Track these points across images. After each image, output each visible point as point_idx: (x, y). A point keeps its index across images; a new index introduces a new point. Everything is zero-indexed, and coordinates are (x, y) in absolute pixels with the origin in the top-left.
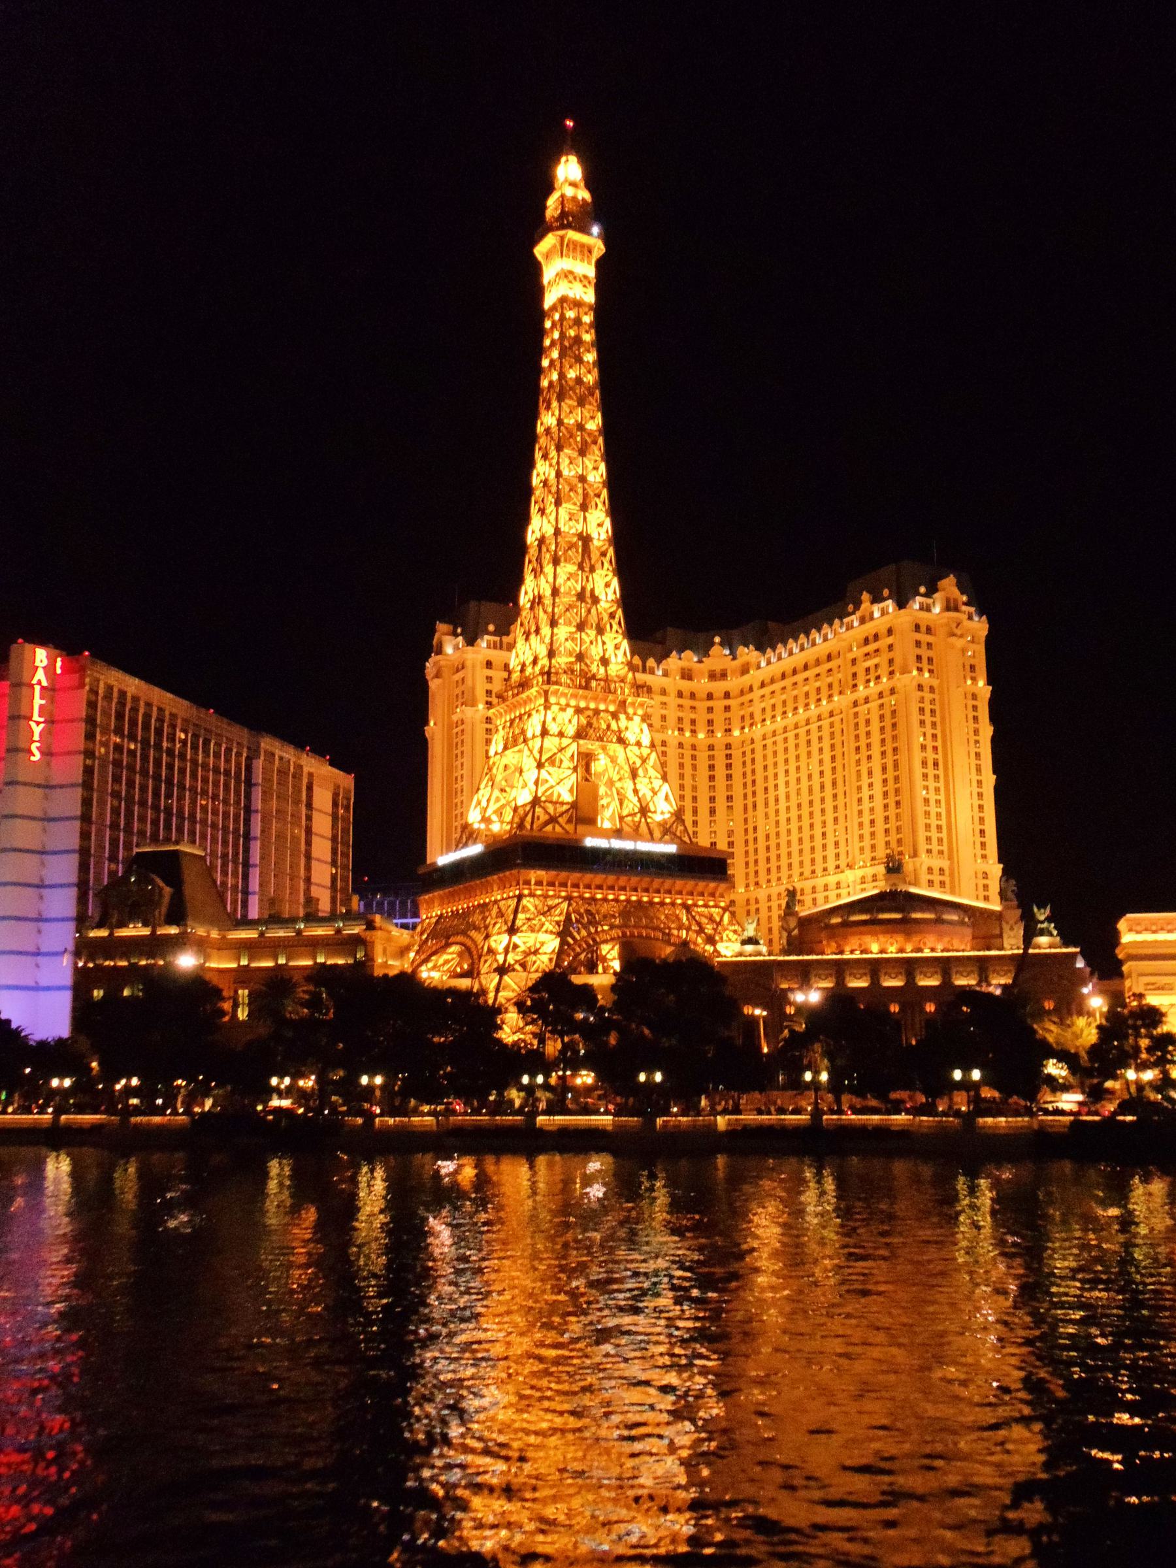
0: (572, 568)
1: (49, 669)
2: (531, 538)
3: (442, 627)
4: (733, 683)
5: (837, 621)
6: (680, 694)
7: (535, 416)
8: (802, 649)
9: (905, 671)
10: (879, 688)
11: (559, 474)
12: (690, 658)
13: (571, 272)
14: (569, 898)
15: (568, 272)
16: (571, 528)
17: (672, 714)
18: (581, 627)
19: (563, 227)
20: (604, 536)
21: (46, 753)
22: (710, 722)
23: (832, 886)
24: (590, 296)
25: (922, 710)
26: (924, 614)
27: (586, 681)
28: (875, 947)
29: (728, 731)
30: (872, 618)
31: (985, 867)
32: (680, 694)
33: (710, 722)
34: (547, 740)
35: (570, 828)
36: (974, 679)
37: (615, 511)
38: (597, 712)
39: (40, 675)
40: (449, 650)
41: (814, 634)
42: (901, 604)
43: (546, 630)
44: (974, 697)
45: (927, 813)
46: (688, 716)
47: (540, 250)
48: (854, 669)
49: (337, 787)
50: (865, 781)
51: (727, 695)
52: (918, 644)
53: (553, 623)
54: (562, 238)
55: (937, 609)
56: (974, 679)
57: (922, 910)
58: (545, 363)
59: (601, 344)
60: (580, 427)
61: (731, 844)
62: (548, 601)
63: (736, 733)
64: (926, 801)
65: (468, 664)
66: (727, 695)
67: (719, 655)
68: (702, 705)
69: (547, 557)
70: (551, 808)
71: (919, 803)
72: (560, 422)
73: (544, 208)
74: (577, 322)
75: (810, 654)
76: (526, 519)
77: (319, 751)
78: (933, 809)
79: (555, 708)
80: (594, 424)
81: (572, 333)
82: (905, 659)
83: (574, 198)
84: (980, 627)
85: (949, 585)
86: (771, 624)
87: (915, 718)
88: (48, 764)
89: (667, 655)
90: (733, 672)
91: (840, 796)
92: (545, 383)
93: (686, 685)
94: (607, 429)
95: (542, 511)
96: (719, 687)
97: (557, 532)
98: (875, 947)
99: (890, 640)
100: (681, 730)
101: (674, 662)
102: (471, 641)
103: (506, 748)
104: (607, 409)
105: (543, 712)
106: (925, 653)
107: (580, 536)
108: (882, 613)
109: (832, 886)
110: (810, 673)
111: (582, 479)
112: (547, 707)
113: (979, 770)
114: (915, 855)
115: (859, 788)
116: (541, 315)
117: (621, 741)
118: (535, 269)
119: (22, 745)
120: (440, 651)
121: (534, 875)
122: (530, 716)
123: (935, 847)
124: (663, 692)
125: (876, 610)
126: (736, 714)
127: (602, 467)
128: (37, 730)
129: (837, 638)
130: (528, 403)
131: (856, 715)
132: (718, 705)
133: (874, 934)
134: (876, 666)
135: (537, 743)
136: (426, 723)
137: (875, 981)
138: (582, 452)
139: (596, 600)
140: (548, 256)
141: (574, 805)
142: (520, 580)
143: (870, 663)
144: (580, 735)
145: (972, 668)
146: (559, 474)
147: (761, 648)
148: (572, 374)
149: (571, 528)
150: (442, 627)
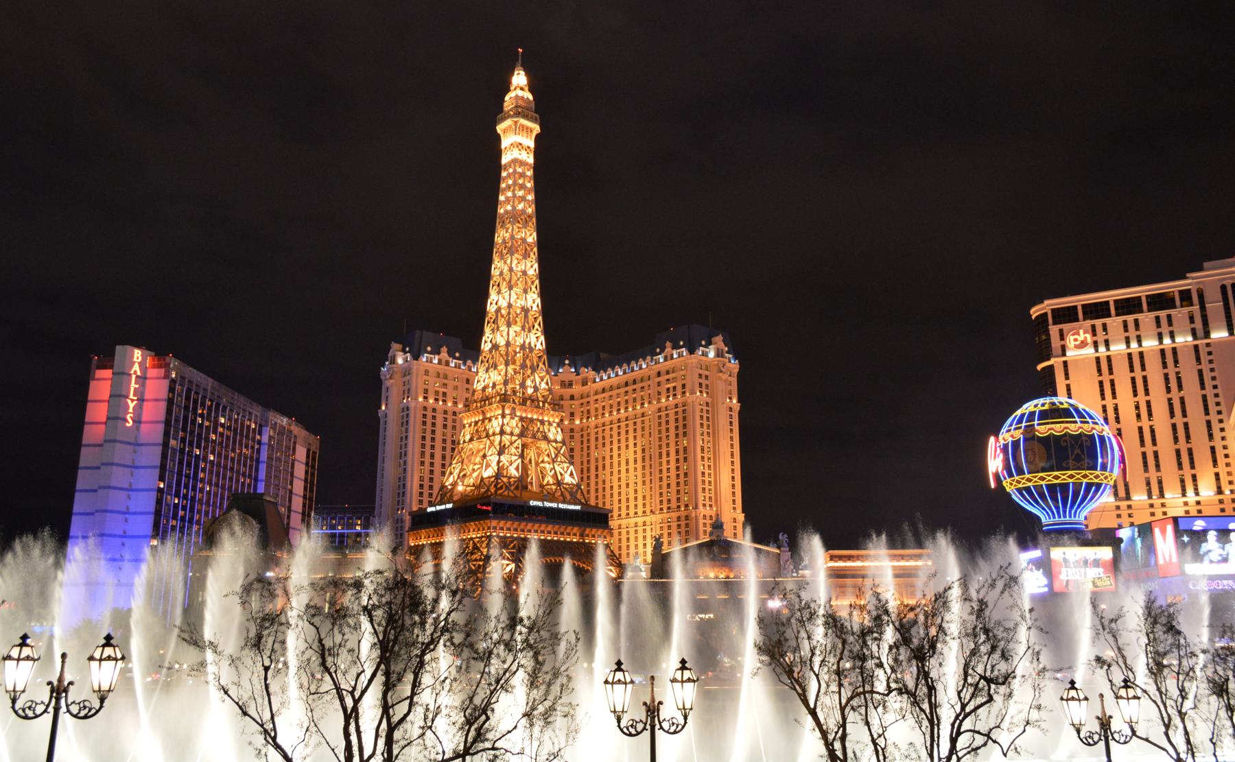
0: (517, 328)
2: (491, 308)
3: (395, 346)
4: (577, 389)
5: (649, 358)
8: (625, 373)
9: (693, 393)
10: (676, 401)
11: (511, 270)
15: (517, 143)
19: (518, 114)
20: (535, 308)
21: (137, 421)
23: (640, 524)
24: (531, 160)
25: (702, 417)
26: (704, 358)
28: (712, 575)
30: (672, 358)
31: (735, 515)
35: (518, 493)
37: (543, 295)
38: (532, 420)
39: (136, 367)
40: (400, 361)
41: (633, 364)
42: (692, 351)
43: (501, 367)
44: (731, 409)
45: (703, 481)
48: (659, 389)
50: (664, 459)
51: (572, 398)
54: (516, 122)
55: (712, 355)
58: (502, 198)
60: (524, 240)
62: (503, 350)
63: (578, 422)
64: (703, 473)
65: (414, 371)
66: (572, 398)
69: (501, 321)
70: (505, 480)
71: (700, 475)
72: (512, 237)
73: (503, 101)
75: (630, 376)
76: (486, 295)
78: (707, 479)
80: (532, 238)
81: (521, 181)
82: (693, 383)
83: (522, 98)
84: (734, 365)
85: (719, 340)
86: (603, 355)
87: (698, 421)
88: (138, 429)
90: (577, 383)
91: (647, 467)
92: (501, 211)
95: (499, 292)
97: (510, 306)
99: (683, 373)
102: (416, 357)
103: (471, 440)
105: (500, 419)
106: (704, 382)
107: (523, 308)
108: (678, 356)
109: (640, 524)
110: (630, 388)
111: (524, 273)
112: (503, 416)
113: (732, 455)
114: (696, 507)
115: (661, 464)
116: (498, 167)
118: (497, 139)
119: (121, 415)
120: (393, 361)
122: (490, 420)
123: (708, 503)
127: (536, 266)
128: (132, 405)
130: (487, 220)
131: (660, 417)
134: (675, 388)
135: (498, 438)
136: (380, 408)
138: (526, 256)
139: (531, 350)
140: (504, 131)
142: (482, 333)
143: (670, 386)
144: (521, 435)
146: (511, 270)
150: (395, 346)
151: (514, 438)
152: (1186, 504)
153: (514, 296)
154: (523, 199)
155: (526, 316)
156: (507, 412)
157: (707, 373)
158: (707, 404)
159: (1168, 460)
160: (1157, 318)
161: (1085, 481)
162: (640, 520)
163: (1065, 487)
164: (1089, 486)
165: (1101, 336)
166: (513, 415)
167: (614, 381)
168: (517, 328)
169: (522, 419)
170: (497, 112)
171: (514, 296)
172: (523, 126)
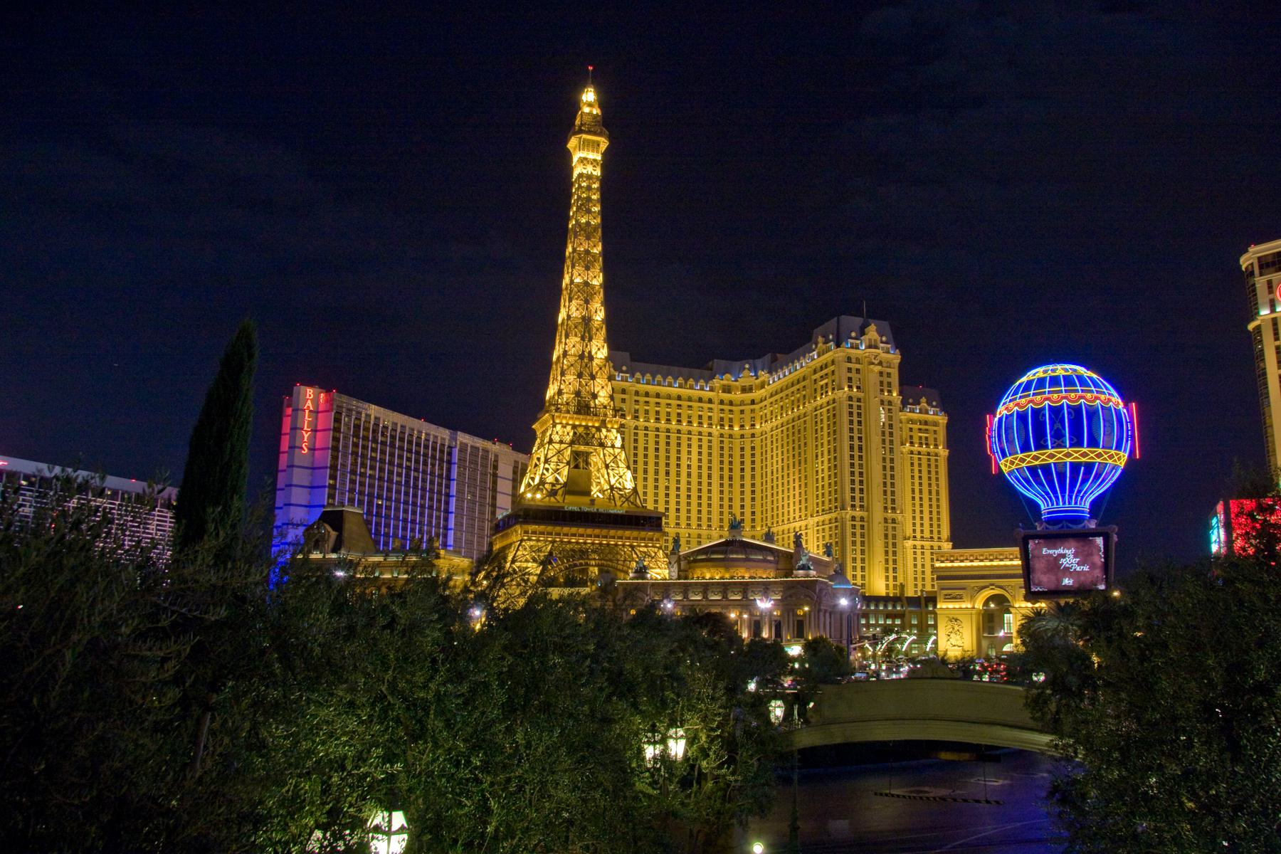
1: (316, 400)
9: (841, 388)
12: (728, 379)
13: (586, 159)
14: (553, 542)
15: (586, 158)
21: (312, 449)
25: (851, 414)
26: (853, 351)
28: (708, 576)
29: (753, 425)
32: (722, 402)
36: (890, 392)
37: (607, 303)
38: (587, 427)
42: (838, 345)
46: (726, 416)
49: (516, 462)
51: (753, 402)
56: (890, 392)
57: (737, 553)
59: (604, 201)
60: (587, 252)
61: (667, 509)
63: (758, 427)
66: (753, 402)
67: (747, 378)
74: (589, 188)
77: (504, 440)
79: (559, 427)
80: (597, 250)
83: (590, 114)
84: (895, 358)
85: (872, 333)
89: (712, 377)
93: (726, 396)
94: (605, 253)
98: (708, 576)
99: (832, 368)
100: (722, 426)
101: (717, 382)
104: (605, 240)
106: (853, 375)
107: (583, 318)
111: (586, 284)
117: (602, 445)
118: (568, 155)
121: (531, 528)
123: (857, 503)
124: (710, 401)
133: (708, 567)
137: (705, 597)
138: (587, 268)
139: (591, 358)
141: (565, 484)
143: (823, 382)
144: (572, 443)
145: (889, 384)
149: (575, 314)
151: (563, 446)
153: (573, 308)
157: (858, 366)
158: (859, 400)
161: (1069, 460)
163: (1046, 469)
164: (1075, 467)
167: (784, 382)
168: (574, 340)
171: (573, 308)
172: (589, 141)
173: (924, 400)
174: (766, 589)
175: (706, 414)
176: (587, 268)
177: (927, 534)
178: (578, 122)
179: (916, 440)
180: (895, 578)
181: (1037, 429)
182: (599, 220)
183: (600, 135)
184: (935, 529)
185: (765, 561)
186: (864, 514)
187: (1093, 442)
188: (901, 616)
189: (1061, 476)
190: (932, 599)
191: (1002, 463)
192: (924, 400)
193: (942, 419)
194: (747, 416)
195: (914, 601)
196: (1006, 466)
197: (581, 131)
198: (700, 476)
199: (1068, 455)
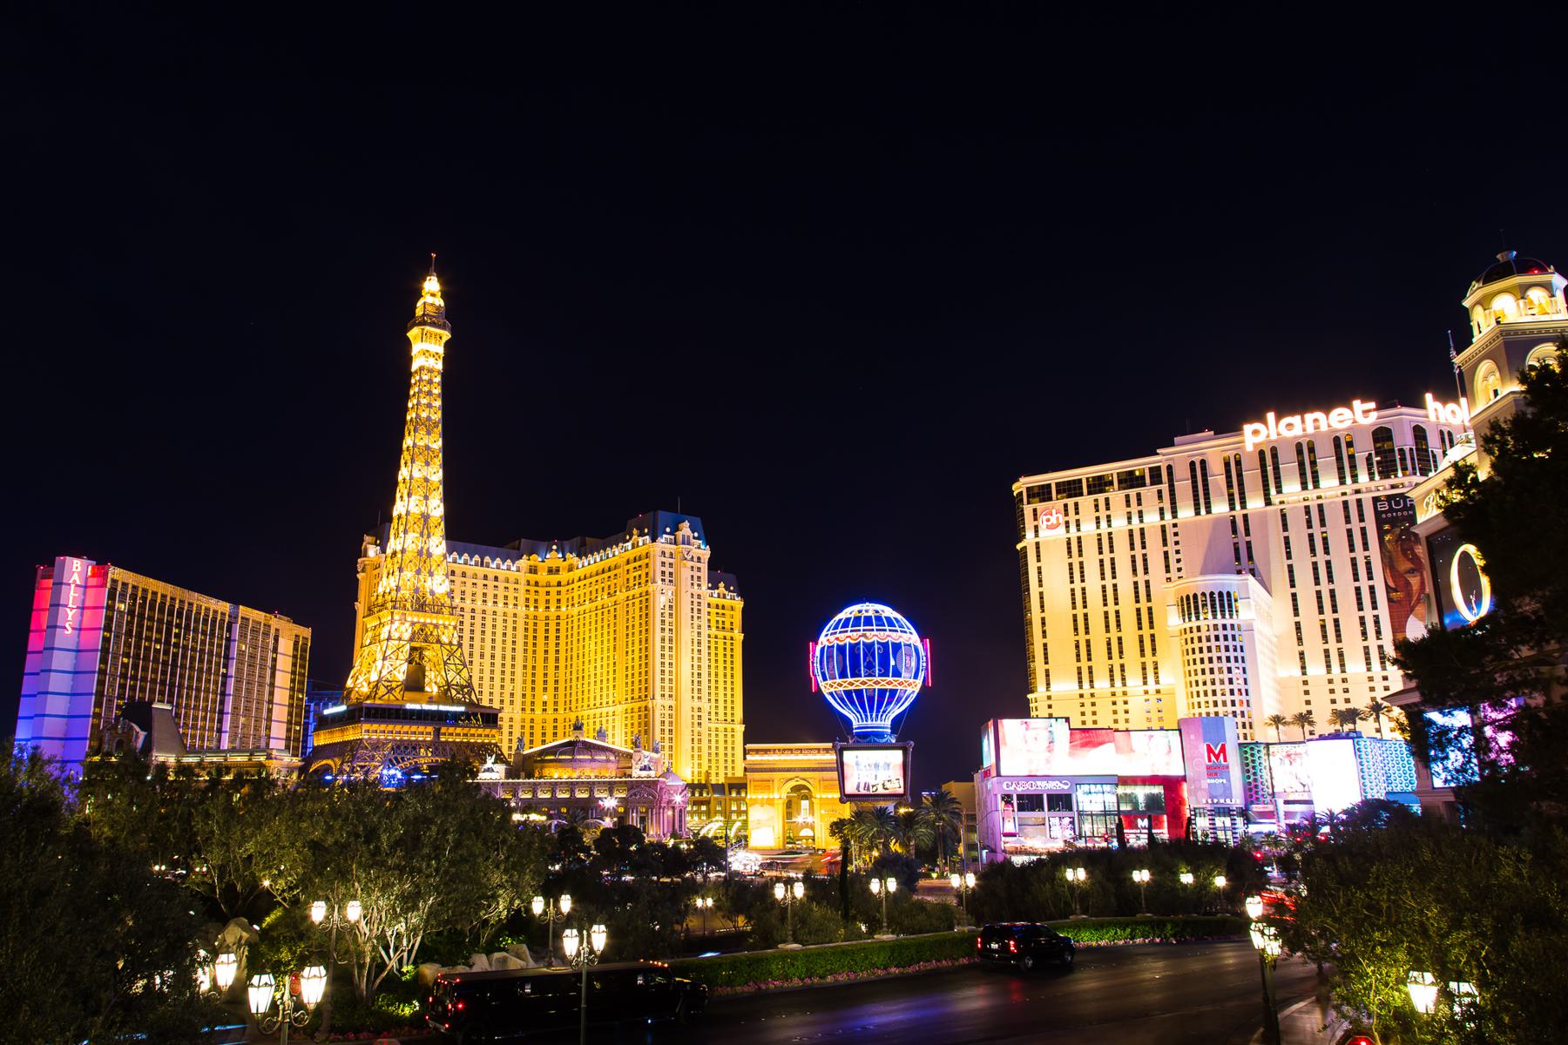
2: (395, 514)
4: (564, 576)
6: (528, 583)
7: (402, 437)
11: (411, 478)
15: (427, 350)
16: (415, 510)
17: (522, 596)
18: (418, 572)
22: (548, 601)
24: (439, 366)
27: (421, 606)
33: (548, 601)
34: (391, 643)
37: (447, 499)
38: (425, 624)
42: (654, 540)
46: (532, 597)
47: (410, 334)
52: (663, 564)
53: (401, 570)
59: (445, 396)
63: (563, 609)
66: (559, 584)
67: (554, 558)
68: (542, 591)
72: (415, 445)
74: (430, 382)
76: (393, 502)
80: (437, 444)
84: (706, 553)
85: (685, 529)
96: (554, 579)
97: (408, 513)
101: (524, 562)
104: (446, 436)
106: (667, 569)
111: (426, 480)
118: (408, 344)
125: (640, 540)
126: (563, 597)
129: (618, 554)
132: (553, 590)
138: (427, 464)
139: (429, 555)
144: (411, 640)
147: (579, 556)
148: (424, 415)
149: (415, 510)
150: (367, 538)
152: (1081, 696)
154: (429, 406)
155: (426, 521)
156: (396, 617)
159: (1131, 646)
160: (1127, 496)
162: (611, 710)
163: (859, 693)
164: (882, 692)
165: (1072, 518)
166: (403, 621)
167: (594, 568)
168: (411, 536)
169: (413, 624)
170: (407, 318)
173: (722, 585)
174: (611, 787)
175: (511, 594)
176: (427, 464)
177: (721, 717)
178: (419, 312)
179: (713, 624)
180: (700, 765)
181: (852, 660)
182: (439, 414)
183: (443, 327)
184: (729, 711)
185: (608, 761)
186: (673, 703)
187: (897, 674)
188: (707, 803)
189: (871, 699)
190: (740, 786)
191: (822, 684)
192: (722, 585)
193: (739, 604)
194: (553, 597)
195: (719, 788)
196: (827, 687)
197: (424, 323)
198: (504, 657)
199: (877, 683)
